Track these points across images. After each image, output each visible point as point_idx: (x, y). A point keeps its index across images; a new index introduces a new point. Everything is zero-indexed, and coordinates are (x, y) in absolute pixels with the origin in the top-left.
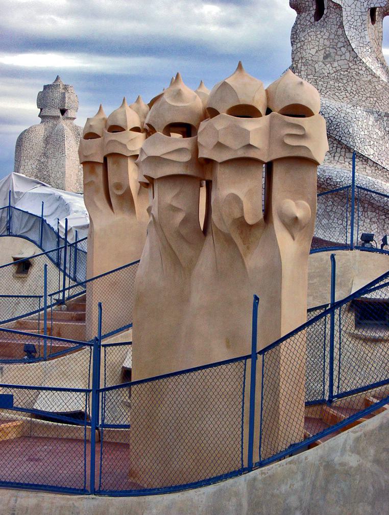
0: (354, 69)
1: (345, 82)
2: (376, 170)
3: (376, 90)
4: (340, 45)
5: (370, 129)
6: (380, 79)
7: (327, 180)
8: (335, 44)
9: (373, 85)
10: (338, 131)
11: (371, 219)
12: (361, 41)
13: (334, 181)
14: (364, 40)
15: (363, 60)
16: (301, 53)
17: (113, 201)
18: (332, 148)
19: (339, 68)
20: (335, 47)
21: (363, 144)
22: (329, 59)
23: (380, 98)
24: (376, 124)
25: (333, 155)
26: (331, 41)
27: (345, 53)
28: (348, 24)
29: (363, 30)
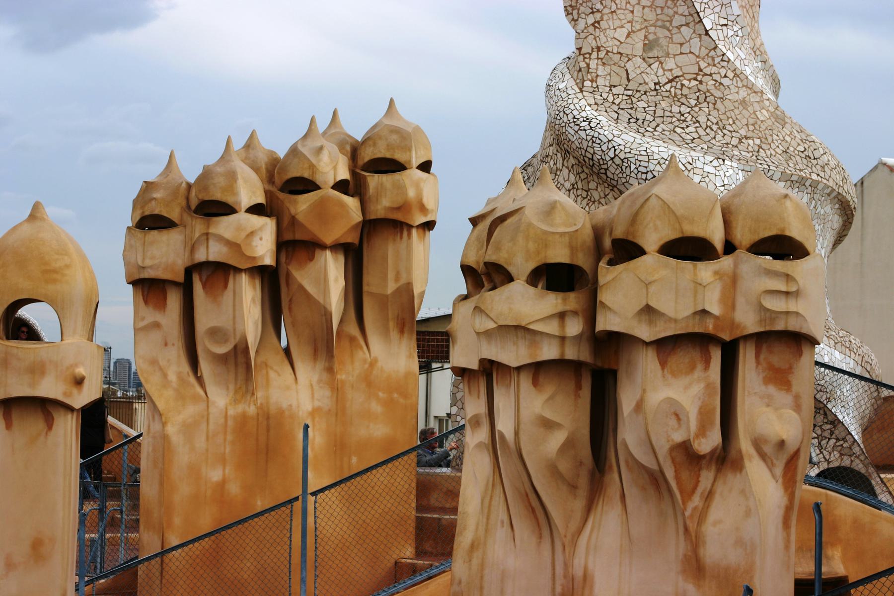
0: (711, 75)
1: (693, 102)
3: (759, 122)
4: (678, 20)
6: (765, 97)
8: (668, 19)
15: (729, 54)
17: (205, 366)
20: (668, 24)
22: (655, 53)
23: (766, 139)
26: (659, 11)
27: (691, 39)
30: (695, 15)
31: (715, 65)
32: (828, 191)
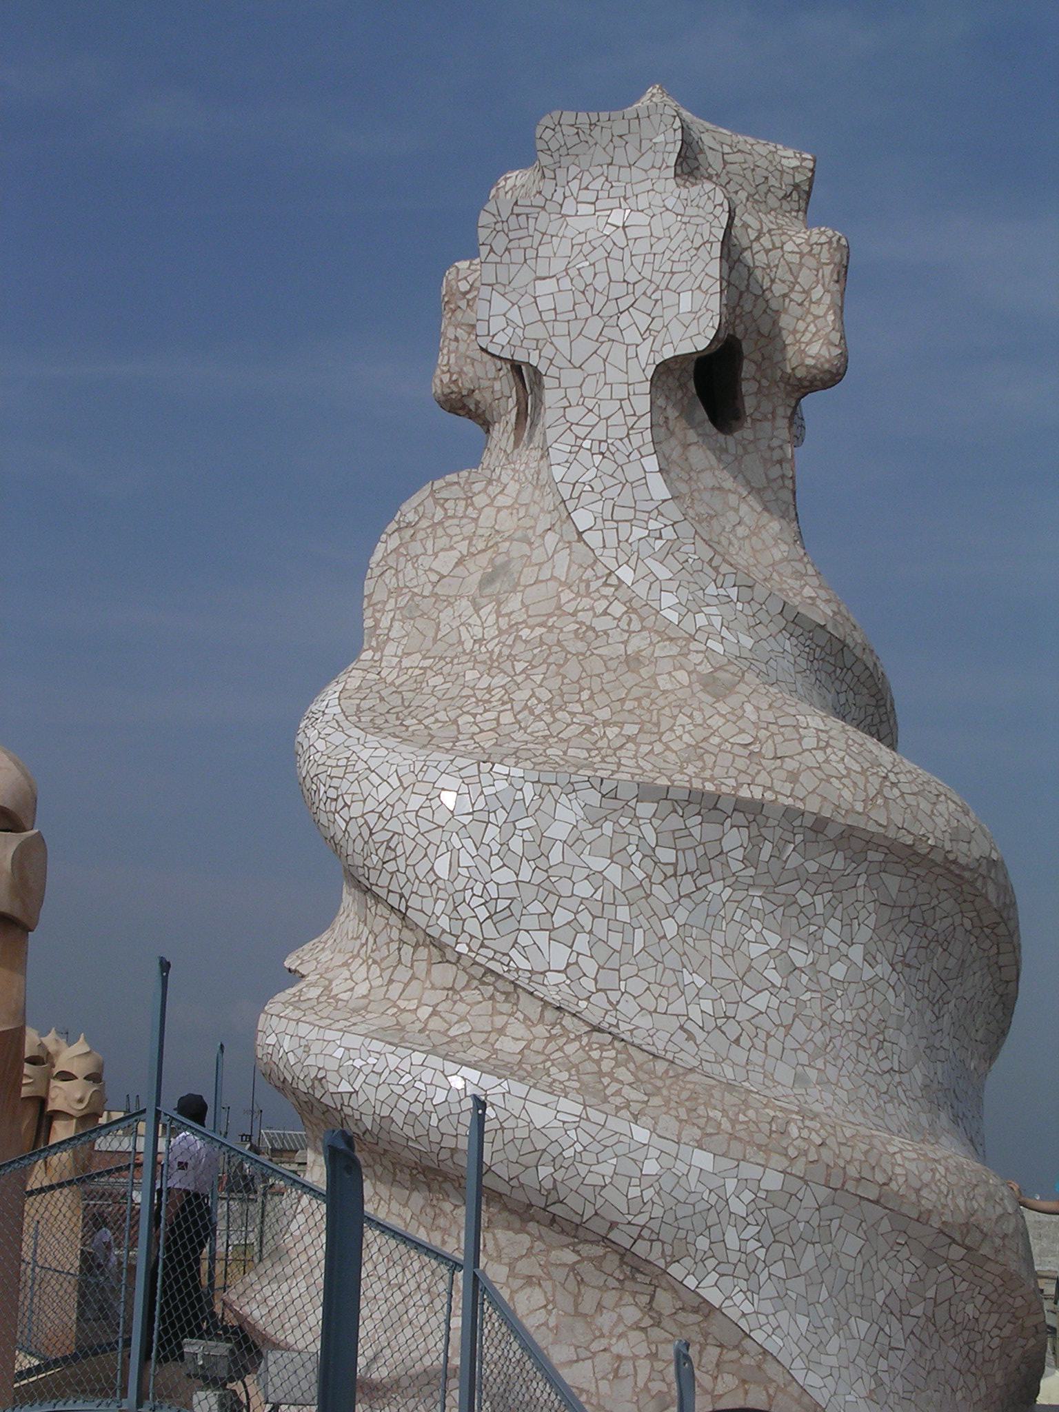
1: (520, 666)
2: (551, 1038)
3: (655, 693)
5: (555, 856)
7: (313, 1087)
9: (645, 672)
10: (392, 873)
11: (512, 1267)
13: (332, 1089)
14: (641, 493)
15: (626, 574)
16: (396, 575)
18: (388, 944)
19: (519, 617)
21: (506, 926)
23: (658, 724)
24: (590, 835)
25: (387, 975)
27: (555, 552)
28: (569, 437)
29: (636, 455)
30: (562, 507)
31: (588, 595)
32: (809, 821)
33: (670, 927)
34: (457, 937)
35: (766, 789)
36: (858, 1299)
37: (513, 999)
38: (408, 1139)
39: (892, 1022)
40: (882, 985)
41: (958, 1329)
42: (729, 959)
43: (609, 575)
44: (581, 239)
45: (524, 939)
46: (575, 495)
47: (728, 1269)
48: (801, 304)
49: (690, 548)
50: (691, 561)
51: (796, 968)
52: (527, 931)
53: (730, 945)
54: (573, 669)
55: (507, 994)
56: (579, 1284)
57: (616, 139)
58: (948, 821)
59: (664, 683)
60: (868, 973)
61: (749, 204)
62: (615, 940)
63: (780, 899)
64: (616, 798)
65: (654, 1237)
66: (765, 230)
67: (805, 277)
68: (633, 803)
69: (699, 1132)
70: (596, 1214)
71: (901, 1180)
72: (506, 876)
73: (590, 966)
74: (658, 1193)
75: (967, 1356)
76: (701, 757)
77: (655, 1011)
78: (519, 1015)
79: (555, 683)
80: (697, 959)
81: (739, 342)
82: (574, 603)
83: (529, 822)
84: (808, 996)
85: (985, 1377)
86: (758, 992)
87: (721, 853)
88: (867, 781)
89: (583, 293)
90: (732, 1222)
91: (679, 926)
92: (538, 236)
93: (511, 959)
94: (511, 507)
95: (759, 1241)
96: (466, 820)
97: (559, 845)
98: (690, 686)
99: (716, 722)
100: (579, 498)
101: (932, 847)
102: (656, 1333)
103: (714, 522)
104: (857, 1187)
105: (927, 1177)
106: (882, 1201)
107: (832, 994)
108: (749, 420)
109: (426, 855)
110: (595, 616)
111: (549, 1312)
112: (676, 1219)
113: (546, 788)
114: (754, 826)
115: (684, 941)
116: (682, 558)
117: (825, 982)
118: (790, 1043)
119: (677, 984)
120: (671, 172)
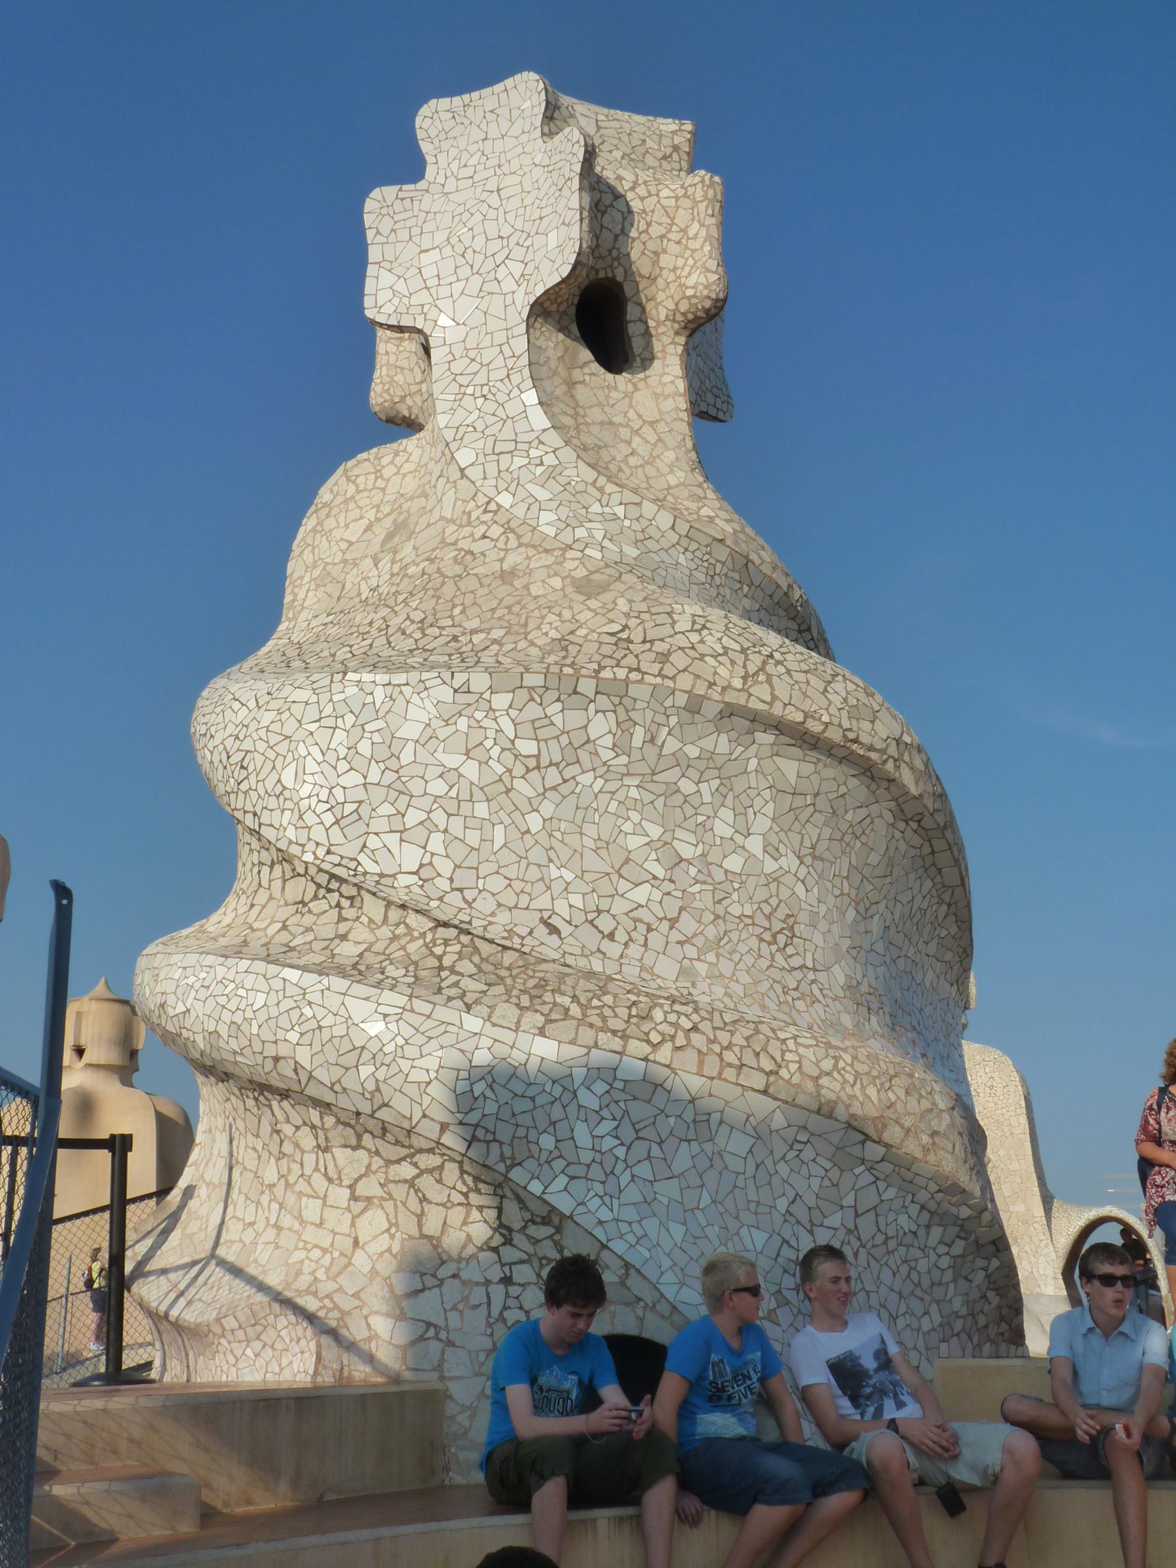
5: (407, 757)
9: (518, 583)
12: (508, 433)
14: (521, 426)
15: (505, 500)
16: (313, 551)
31: (469, 524)
32: (681, 699)
33: (534, 822)
34: (303, 846)
35: (631, 670)
36: (753, 1206)
37: (357, 903)
38: (235, 1052)
39: (803, 917)
40: (789, 880)
41: (892, 1244)
42: (603, 853)
43: (488, 503)
44: (461, 209)
45: (373, 842)
46: (459, 436)
47: (578, 1170)
48: (679, 242)
49: (571, 472)
50: (573, 483)
51: (682, 860)
52: (376, 834)
53: (605, 837)
54: (448, 591)
55: (351, 898)
56: (421, 1202)
57: (488, 115)
58: (845, 700)
59: (535, 590)
60: (770, 866)
61: (624, 162)
62: (473, 838)
63: (661, 789)
64: (469, 692)
65: (490, 1137)
66: (641, 181)
67: (682, 218)
68: (487, 696)
69: (542, 1019)
70: (424, 1116)
71: (794, 1067)
72: (354, 779)
73: (445, 867)
74: (491, 1087)
75: (908, 1276)
76: (565, 649)
77: (516, 907)
78: (364, 919)
79: (429, 605)
80: (565, 853)
81: (620, 286)
82: (456, 535)
83: (380, 724)
84: (697, 888)
85: (938, 1302)
86: (637, 885)
87: (588, 741)
88: (747, 659)
89: (463, 256)
90: (582, 1117)
91: (544, 820)
92: (422, 216)
93: (359, 864)
94: (416, 470)
95: (617, 1137)
96: (313, 727)
97: (411, 744)
98: (563, 589)
99: (585, 616)
100: (462, 439)
101: (827, 724)
102: (509, 1254)
103: (603, 452)
104: (738, 1074)
105: (827, 1065)
106: (771, 1090)
107: (727, 887)
108: (638, 359)
109: (274, 767)
110: (474, 540)
111: (392, 1237)
112: (514, 1115)
113: (397, 689)
114: (620, 709)
115: (550, 835)
116: (563, 480)
117: (719, 875)
118: (675, 936)
119: (542, 879)
120: (538, 132)
